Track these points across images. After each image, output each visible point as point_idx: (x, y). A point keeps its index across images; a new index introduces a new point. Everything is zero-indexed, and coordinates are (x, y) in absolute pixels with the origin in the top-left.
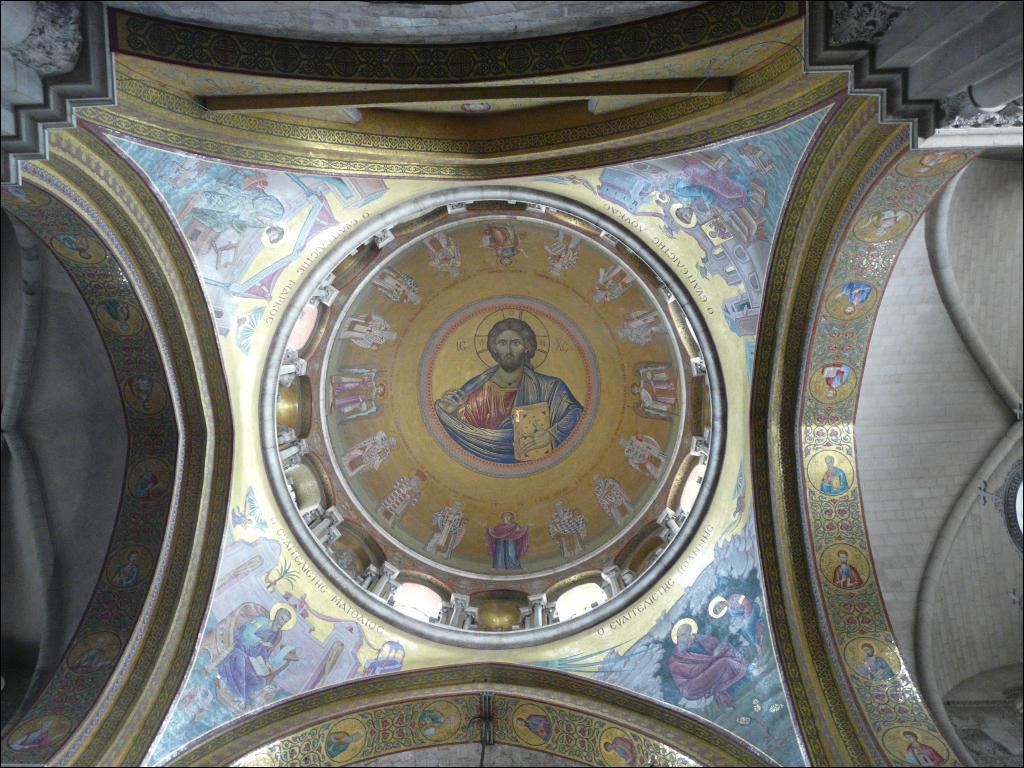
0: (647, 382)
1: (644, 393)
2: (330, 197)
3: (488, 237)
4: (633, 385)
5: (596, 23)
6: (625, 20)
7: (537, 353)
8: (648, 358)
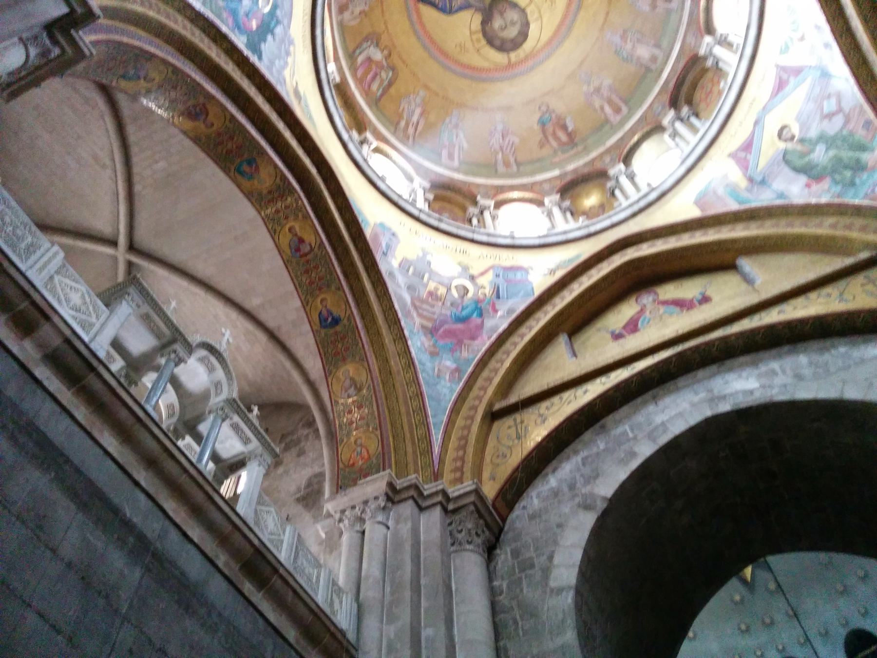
0: (382, 67)
1: (377, 55)
2: (743, 183)
3: (570, 129)
4: (390, 55)
5: (603, 427)
6: (587, 436)
7: (479, 27)
8: (392, 91)
